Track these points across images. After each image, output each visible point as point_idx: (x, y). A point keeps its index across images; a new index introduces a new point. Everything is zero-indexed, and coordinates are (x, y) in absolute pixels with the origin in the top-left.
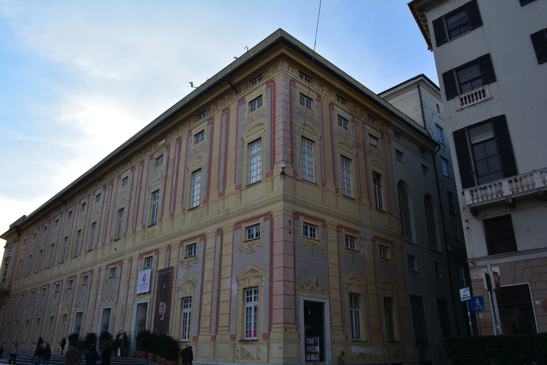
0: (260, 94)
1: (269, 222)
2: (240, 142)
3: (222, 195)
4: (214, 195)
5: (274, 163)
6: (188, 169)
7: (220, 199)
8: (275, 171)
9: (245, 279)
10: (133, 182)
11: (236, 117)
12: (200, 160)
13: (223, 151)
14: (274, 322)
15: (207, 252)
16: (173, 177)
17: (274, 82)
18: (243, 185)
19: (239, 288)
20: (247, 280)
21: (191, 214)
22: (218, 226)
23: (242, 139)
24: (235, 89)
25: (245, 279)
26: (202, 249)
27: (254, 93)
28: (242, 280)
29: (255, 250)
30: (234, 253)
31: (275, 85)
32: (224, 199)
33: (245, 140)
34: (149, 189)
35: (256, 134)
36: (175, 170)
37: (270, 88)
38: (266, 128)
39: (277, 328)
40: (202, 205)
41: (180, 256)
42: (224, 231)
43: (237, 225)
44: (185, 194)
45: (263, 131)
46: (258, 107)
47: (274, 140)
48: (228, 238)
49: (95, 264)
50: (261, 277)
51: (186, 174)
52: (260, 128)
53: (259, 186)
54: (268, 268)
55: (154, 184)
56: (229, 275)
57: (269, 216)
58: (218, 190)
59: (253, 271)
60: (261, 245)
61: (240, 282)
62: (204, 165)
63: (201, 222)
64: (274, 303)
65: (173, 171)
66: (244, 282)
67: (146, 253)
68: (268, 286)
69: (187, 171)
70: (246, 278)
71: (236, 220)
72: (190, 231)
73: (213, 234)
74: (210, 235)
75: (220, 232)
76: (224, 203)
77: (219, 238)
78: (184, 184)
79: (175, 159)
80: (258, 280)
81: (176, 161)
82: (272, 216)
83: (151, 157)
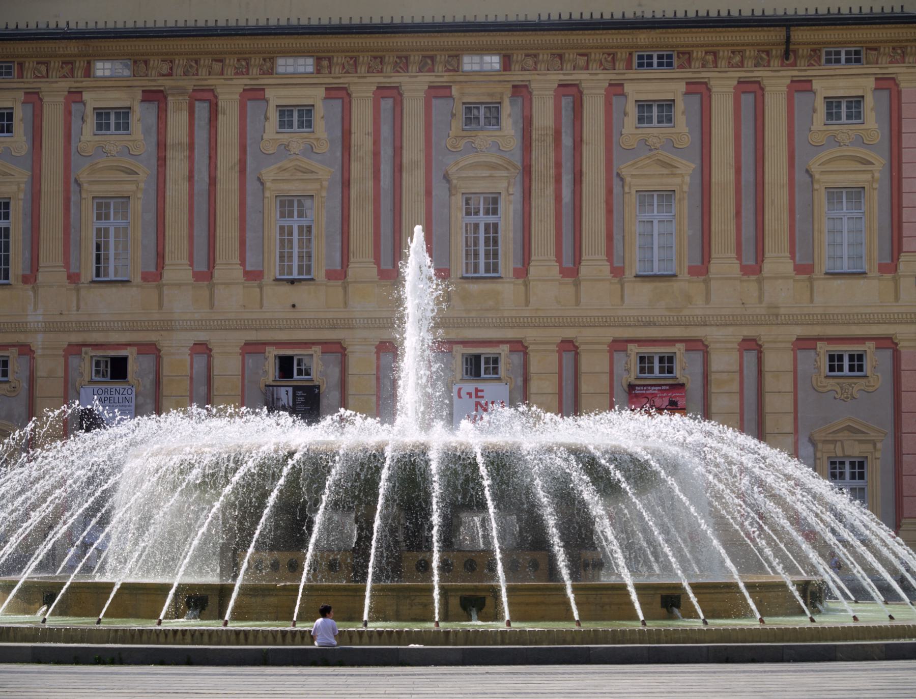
0: (860, 94)
1: (889, 353)
2: (800, 176)
3: (753, 269)
4: (724, 262)
5: (900, 251)
6: (622, 180)
7: (745, 277)
8: (902, 267)
9: (834, 442)
10: (346, 135)
11: (785, 115)
12: (665, 171)
13: (748, 175)
14: (906, 514)
15: (713, 377)
16: (558, 180)
17: (897, 85)
18: (816, 269)
19: (819, 455)
20: (839, 444)
21: (647, 288)
22: (748, 332)
23: (807, 171)
24: (788, 53)
25: (834, 442)
26: (698, 369)
27: (842, 83)
28: (825, 442)
29: (857, 395)
30: (800, 395)
31: (899, 92)
32: (760, 282)
33: (817, 176)
34: (446, 178)
35: (852, 177)
36: (567, 166)
37: (885, 94)
38: (877, 175)
39: (912, 524)
40: (684, 275)
41: (619, 369)
42: (766, 346)
43: (805, 343)
44: (617, 237)
45: (868, 176)
46: (849, 117)
47: (900, 207)
48: (778, 361)
49: (167, 326)
50: (875, 444)
51: (616, 189)
52: (863, 167)
53: (862, 282)
54: (889, 429)
55: (471, 173)
56: (790, 428)
57: (887, 343)
58: (739, 257)
59: (849, 429)
60: (871, 389)
61: (820, 446)
62: (685, 188)
63: (686, 312)
64: (905, 487)
65: (558, 165)
66: (832, 446)
67: (465, 343)
68: (890, 458)
69: (616, 181)
70: (836, 441)
71: (799, 331)
72: (649, 324)
73: (729, 346)
74: (718, 345)
75: (751, 345)
76: (761, 290)
77: (750, 358)
78: (609, 211)
79: (558, 134)
80: (869, 447)
81: (567, 141)
82: (896, 344)
83: (438, 92)
